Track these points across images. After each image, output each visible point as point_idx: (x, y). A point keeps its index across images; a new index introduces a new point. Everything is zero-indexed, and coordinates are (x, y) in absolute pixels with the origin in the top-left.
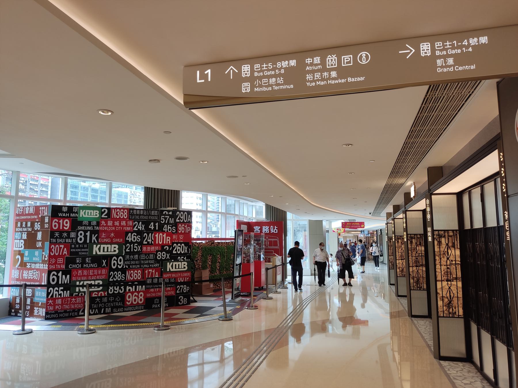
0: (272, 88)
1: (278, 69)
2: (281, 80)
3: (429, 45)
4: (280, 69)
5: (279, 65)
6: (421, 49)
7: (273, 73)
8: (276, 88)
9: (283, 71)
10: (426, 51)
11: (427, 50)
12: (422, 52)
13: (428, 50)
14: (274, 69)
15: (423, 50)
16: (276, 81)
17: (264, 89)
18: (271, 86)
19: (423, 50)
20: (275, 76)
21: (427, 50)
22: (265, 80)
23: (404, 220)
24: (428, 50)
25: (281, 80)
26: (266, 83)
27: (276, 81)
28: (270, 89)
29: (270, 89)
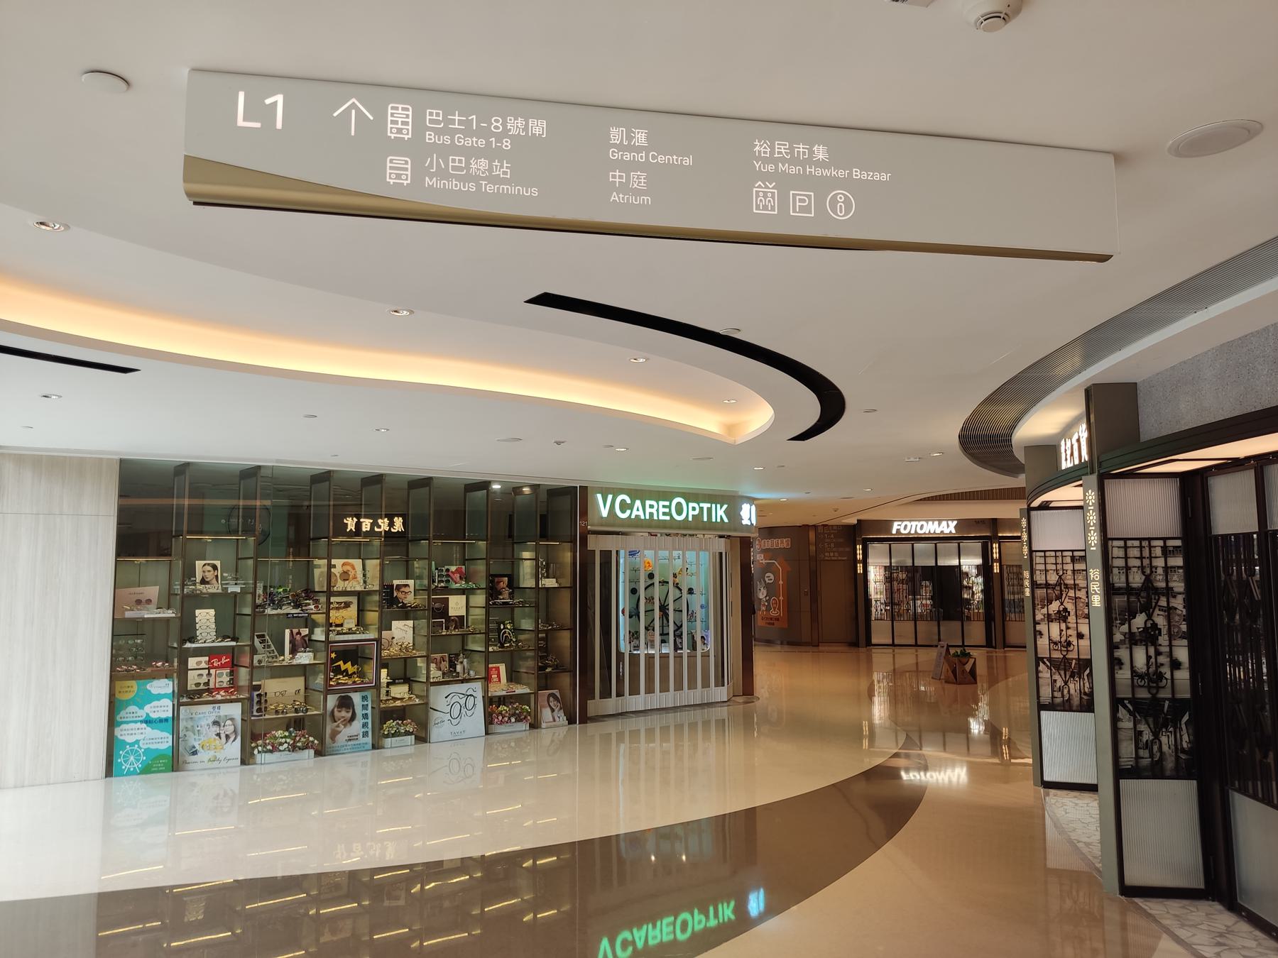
0: (479, 186)
1: (494, 135)
2: (503, 169)
3: (410, 113)
4: (499, 137)
5: (496, 124)
6: (390, 118)
7: (482, 143)
8: (490, 188)
9: (507, 144)
10: (400, 126)
11: (403, 123)
12: (389, 126)
13: (407, 124)
14: (484, 133)
15: (393, 122)
16: (490, 169)
17: (454, 185)
18: (476, 179)
19: (393, 122)
20: (491, 154)
21: (403, 123)
22: (456, 161)
23: (1093, 518)
24: (407, 124)
25: (503, 169)
26: (460, 169)
27: (490, 169)
28: (472, 187)
29: (472, 187)
